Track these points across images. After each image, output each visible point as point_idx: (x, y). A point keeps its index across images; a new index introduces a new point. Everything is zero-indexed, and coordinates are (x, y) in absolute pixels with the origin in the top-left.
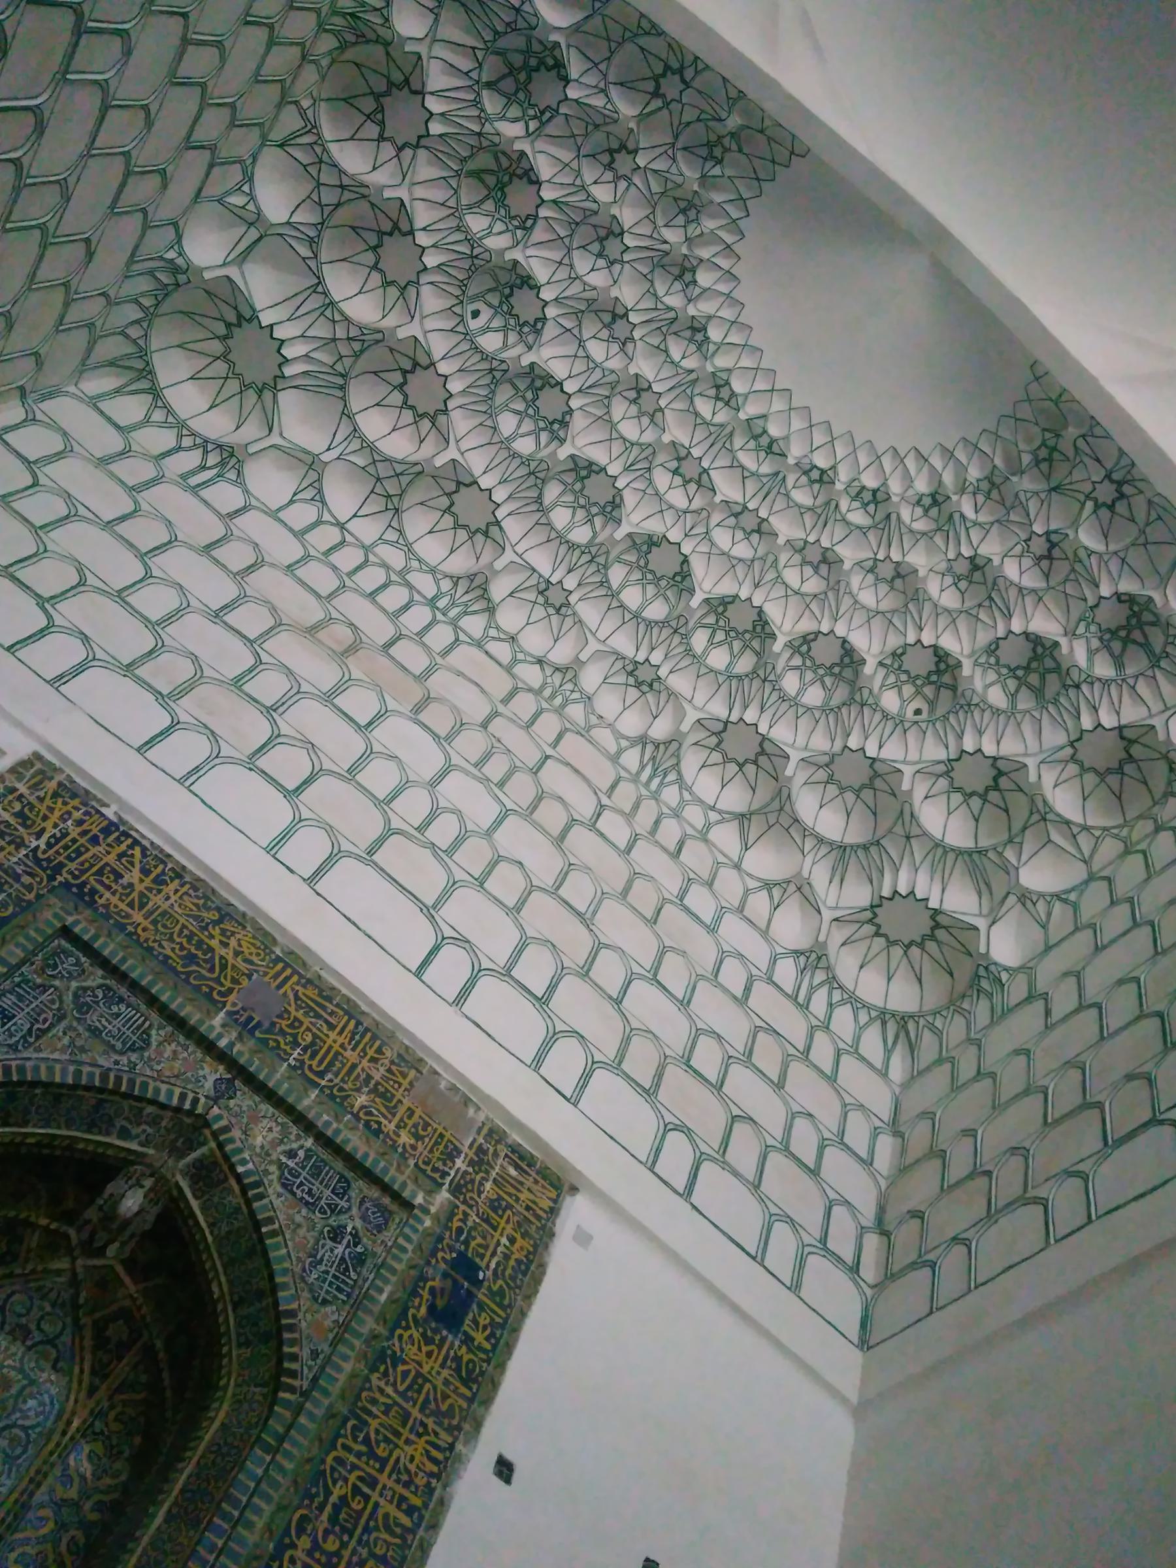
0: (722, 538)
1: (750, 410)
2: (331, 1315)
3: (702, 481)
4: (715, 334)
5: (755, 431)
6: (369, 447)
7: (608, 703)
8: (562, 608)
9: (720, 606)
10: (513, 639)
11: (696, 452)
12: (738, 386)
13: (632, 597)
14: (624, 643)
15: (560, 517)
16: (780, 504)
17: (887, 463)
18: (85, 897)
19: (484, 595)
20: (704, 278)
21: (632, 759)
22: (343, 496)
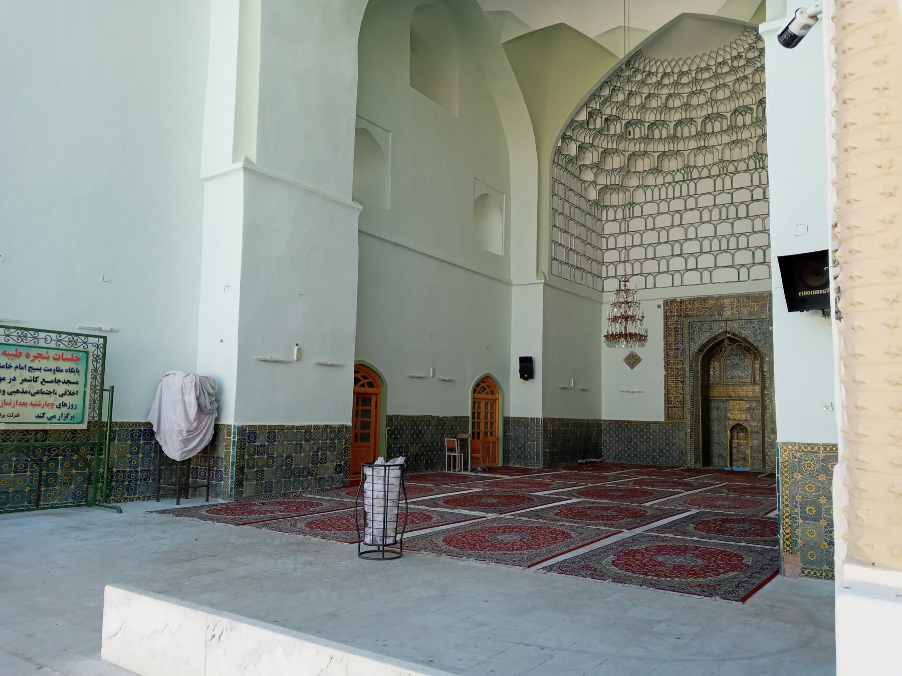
0: (720, 95)
1: (694, 67)
2: (763, 342)
3: (702, 91)
4: (669, 70)
5: (700, 70)
6: (644, 172)
7: (737, 153)
8: (706, 147)
9: (736, 110)
10: (705, 166)
11: (694, 89)
12: (685, 69)
13: (717, 128)
14: (726, 139)
15: (686, 134)
16: (723, 76)
17: (734, 46)
18: (687, 316)
19: (691, 167)
20: (654, 70)
21: (752, 165)
22: (650, 180)
